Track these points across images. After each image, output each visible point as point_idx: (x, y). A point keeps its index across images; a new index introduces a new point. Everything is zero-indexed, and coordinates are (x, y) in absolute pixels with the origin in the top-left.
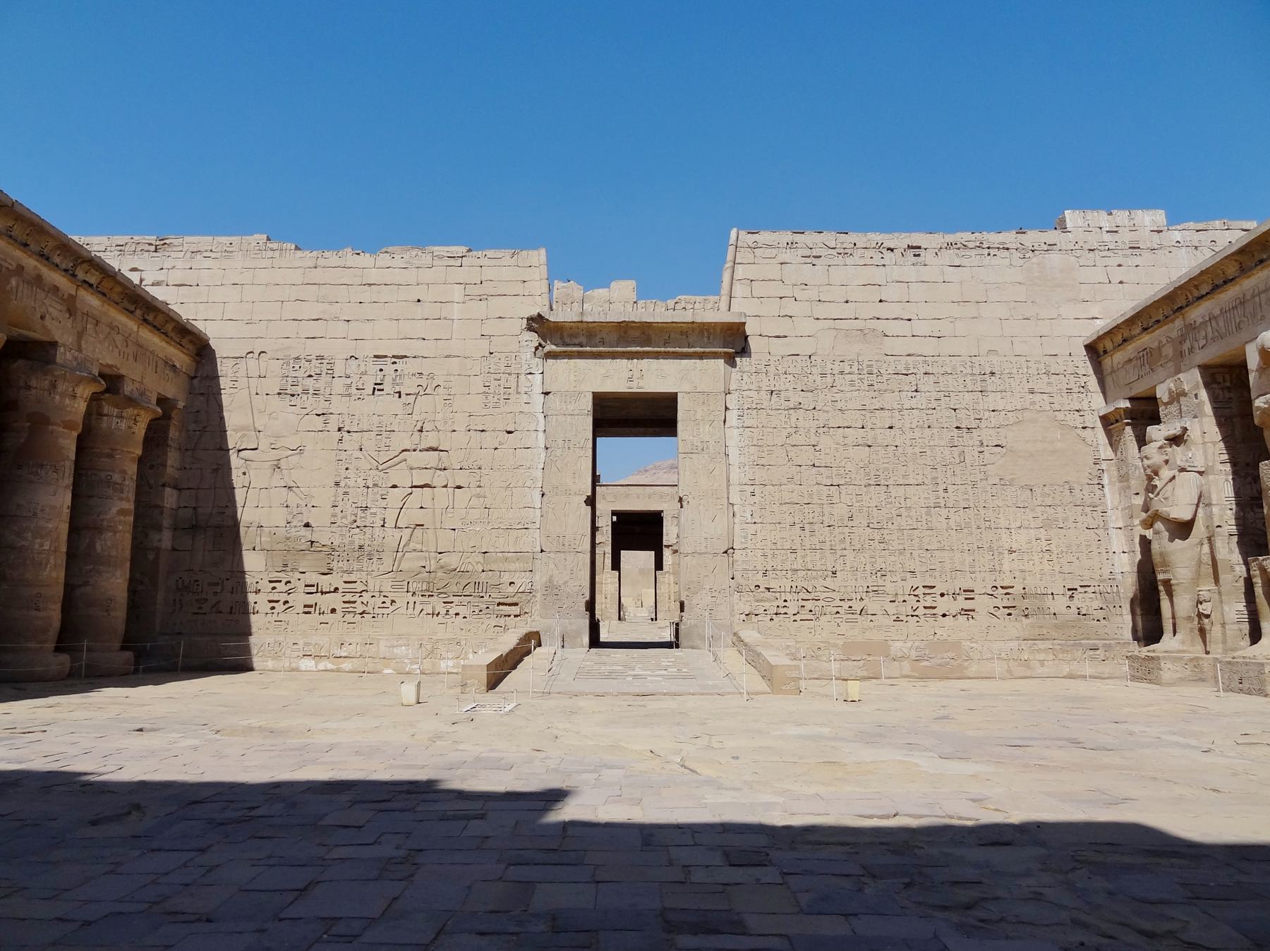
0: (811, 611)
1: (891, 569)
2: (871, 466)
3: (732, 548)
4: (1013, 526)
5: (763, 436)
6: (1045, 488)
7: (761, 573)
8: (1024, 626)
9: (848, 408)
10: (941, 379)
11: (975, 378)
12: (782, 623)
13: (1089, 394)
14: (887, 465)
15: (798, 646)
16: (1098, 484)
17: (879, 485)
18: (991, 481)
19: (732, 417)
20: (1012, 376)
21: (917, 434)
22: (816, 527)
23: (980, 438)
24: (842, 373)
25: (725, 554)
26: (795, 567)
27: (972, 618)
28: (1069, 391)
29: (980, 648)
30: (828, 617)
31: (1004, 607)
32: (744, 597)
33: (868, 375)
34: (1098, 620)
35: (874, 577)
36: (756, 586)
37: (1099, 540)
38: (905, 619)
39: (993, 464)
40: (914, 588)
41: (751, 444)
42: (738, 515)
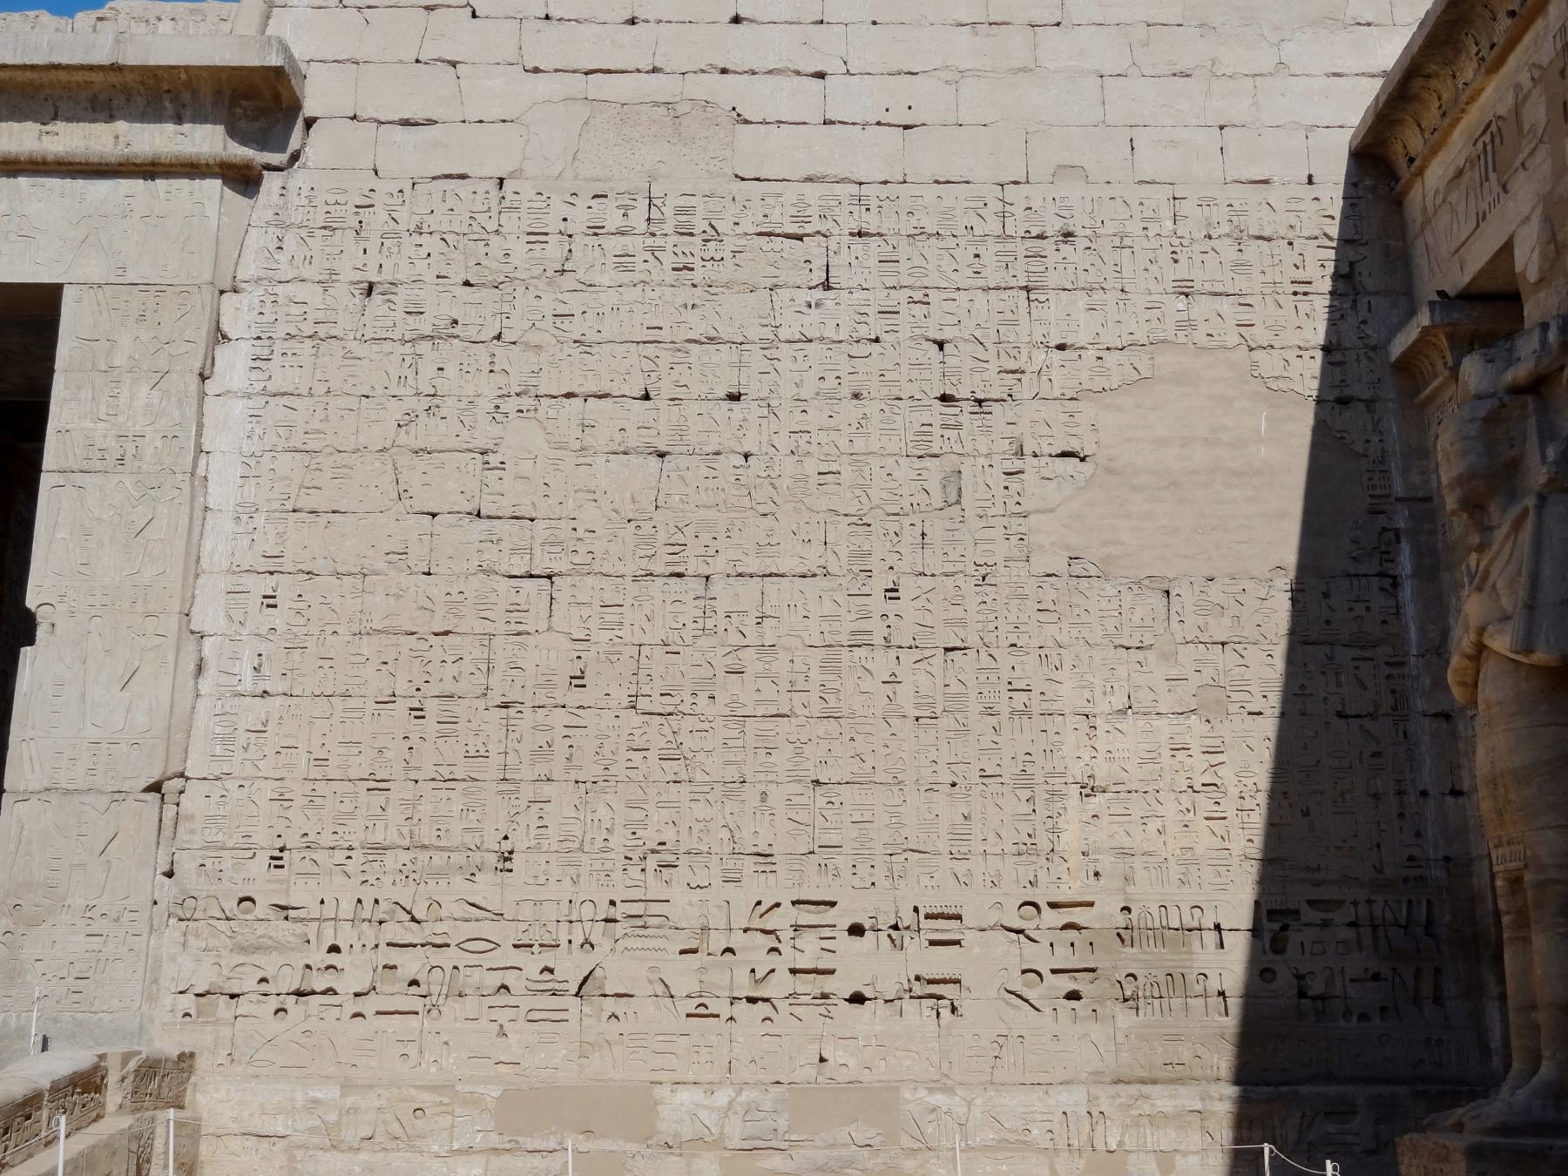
0: (414, 983)
1: (692, 844)
2: (659, 517)
3: (182, 775)
4: (1102, 706)
5: (326, 419)
6: (1214, 590)
7: (263, 858)
8: (1120, 1039)
9: (606, 335)
10: (904, 251)
11: (1010, 247)
12: (314, 1024)
13: (1363, 302)
14: (712, 514)
15: (350, 1101)
16: (1381, 575)
17: (680, 575)
18: (1040, 564)
19: (233, 365)
20: (1127, 242)
21: (816, 417)
22: (459, 708)
23: (1010, 431)
24: (596, 230)
25: (153, 797)
26: (378, 837)
27: (954, 1010)
28: (1301, 288)
29: (962, 1110)
30: (471, 1002)
31: (1054, 971)
32: (197, 936)
33: (677, 239)
34: (1363, 1017)
35: (634, 872)
36: (242, 900)
37: (1375, 755)
38: (725, 1010)
39: (1051, 511)
40: (763, 908)
41: (282, 444)
42: (211, 671)
